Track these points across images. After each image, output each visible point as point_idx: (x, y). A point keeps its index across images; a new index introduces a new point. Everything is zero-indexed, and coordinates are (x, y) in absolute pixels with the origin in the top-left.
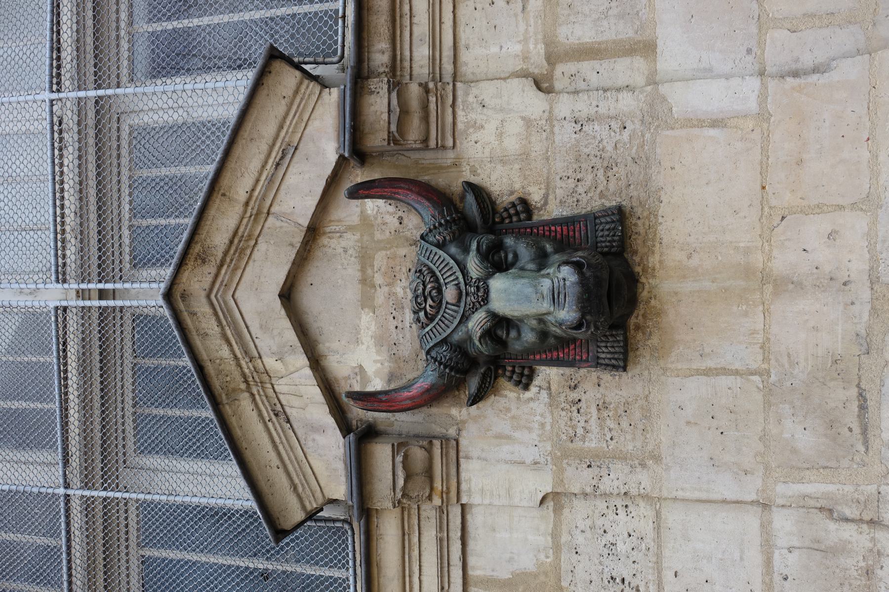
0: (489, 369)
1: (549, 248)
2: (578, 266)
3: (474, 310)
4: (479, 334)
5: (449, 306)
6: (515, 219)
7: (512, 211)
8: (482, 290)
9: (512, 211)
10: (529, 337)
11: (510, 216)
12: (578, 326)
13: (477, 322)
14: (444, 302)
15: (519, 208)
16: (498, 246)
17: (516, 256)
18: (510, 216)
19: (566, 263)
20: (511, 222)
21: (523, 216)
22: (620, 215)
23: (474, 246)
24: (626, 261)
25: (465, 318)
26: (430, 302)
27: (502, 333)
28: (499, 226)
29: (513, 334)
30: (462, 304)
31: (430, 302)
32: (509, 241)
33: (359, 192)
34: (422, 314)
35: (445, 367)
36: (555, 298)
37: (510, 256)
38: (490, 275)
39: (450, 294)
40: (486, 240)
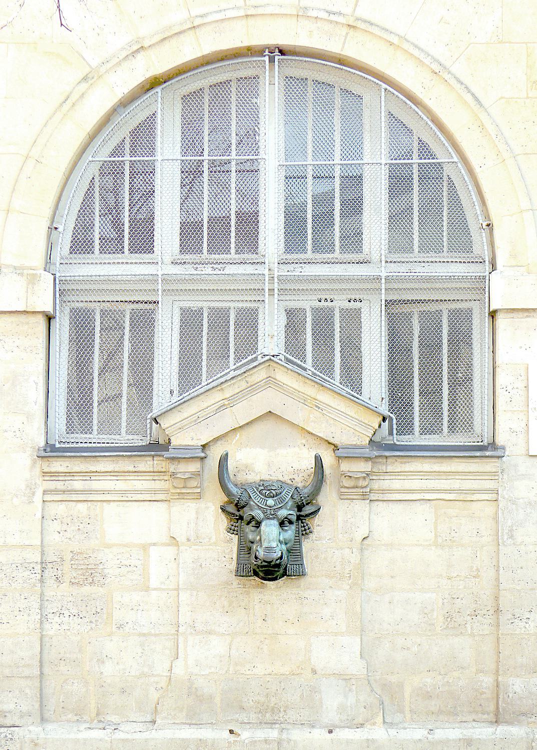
0: (237, 516)
1: (288, 545)
2: (281, 558)
3: (264, 513)
4: (253, 514)
5: (266, 501)
6: (303, 529)
7: (307, 527)
8: (272, 517)
9: (307, 527)
10: (251, 537)
11: (304, 526)
12: (256, 558)
13: (258, 514)
14: (267, 499)
15: (308, 531)
16: (291, 522)
17: (286, 531)
18: (304, 526)
19: (282, 553)
20: (302, 527)
21: (304, 532)
22: (302, 574)
23: (291, 512)
24: (283, 576)
25: (260, 508)
26: (268, 492)
27: (253, 523)
28: (300, 522)
29: (253, 529)
30: (266, 507)
31: (268, 492)
32: (293, 527)
33: (318, 461)
34: (262, 488)
35: (239, 498)
36: (269, 549)
37: (286, 528)
38: (278, 519)
39: (271, 502)
40: (294, 518)
